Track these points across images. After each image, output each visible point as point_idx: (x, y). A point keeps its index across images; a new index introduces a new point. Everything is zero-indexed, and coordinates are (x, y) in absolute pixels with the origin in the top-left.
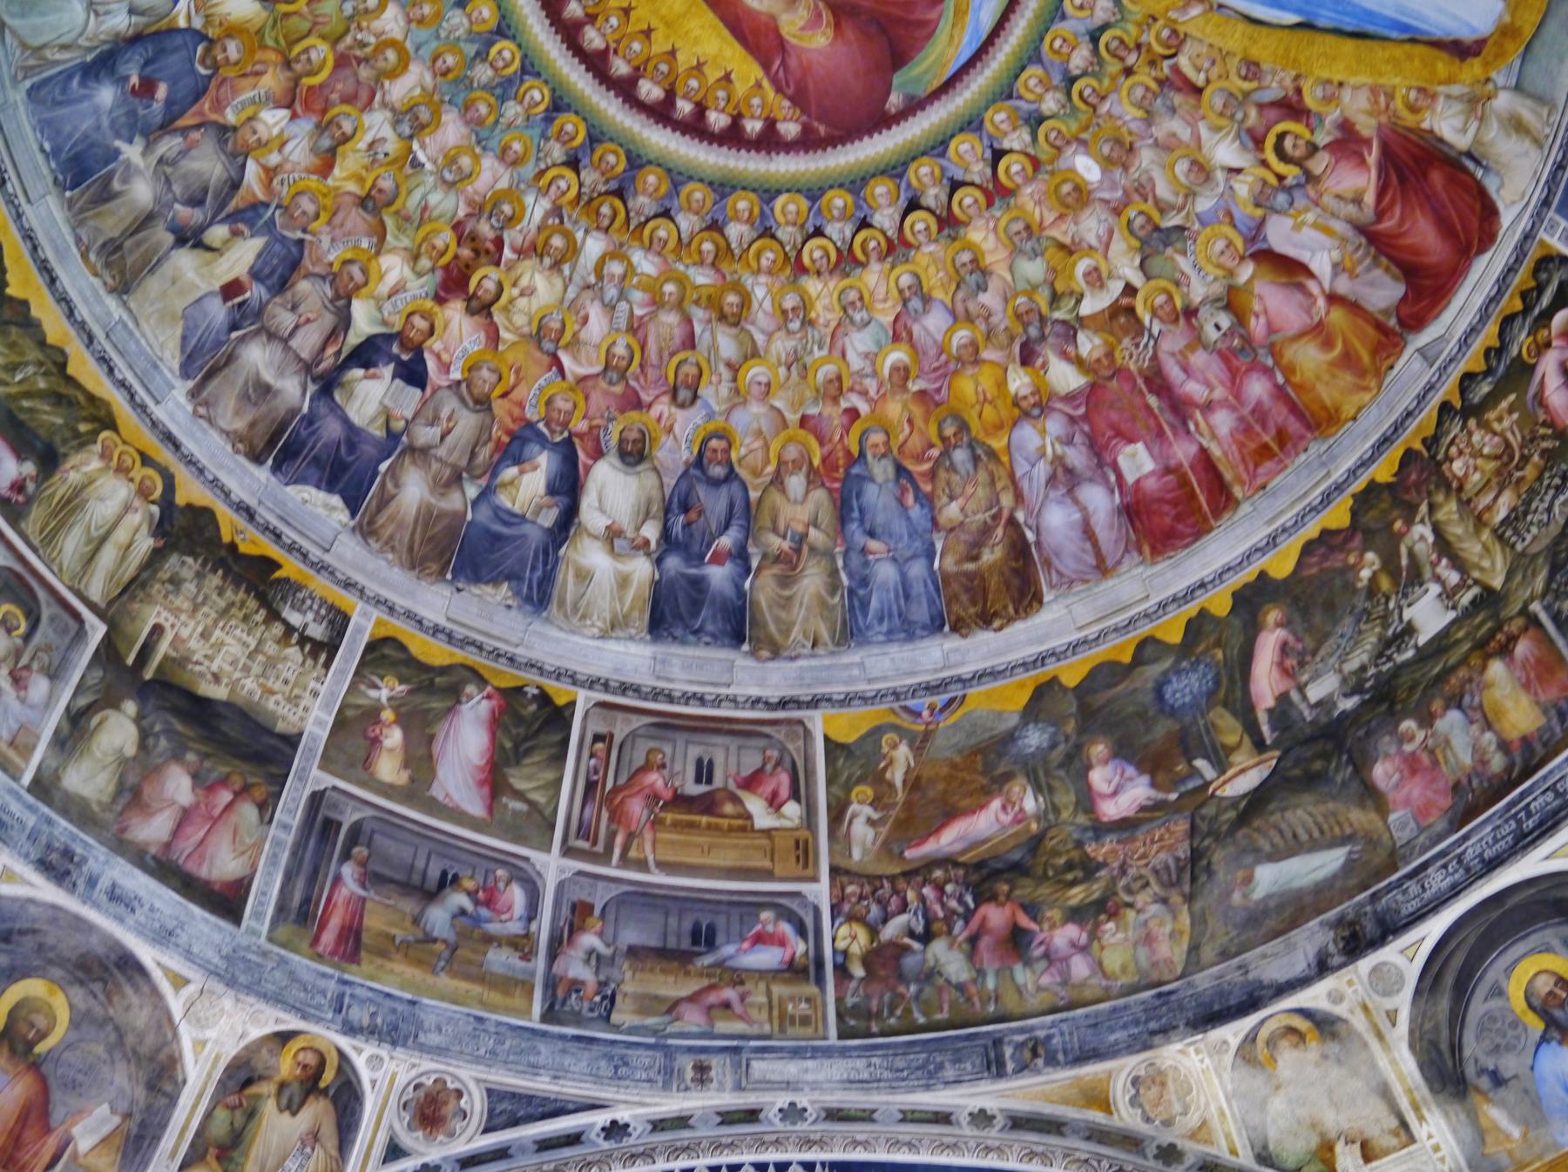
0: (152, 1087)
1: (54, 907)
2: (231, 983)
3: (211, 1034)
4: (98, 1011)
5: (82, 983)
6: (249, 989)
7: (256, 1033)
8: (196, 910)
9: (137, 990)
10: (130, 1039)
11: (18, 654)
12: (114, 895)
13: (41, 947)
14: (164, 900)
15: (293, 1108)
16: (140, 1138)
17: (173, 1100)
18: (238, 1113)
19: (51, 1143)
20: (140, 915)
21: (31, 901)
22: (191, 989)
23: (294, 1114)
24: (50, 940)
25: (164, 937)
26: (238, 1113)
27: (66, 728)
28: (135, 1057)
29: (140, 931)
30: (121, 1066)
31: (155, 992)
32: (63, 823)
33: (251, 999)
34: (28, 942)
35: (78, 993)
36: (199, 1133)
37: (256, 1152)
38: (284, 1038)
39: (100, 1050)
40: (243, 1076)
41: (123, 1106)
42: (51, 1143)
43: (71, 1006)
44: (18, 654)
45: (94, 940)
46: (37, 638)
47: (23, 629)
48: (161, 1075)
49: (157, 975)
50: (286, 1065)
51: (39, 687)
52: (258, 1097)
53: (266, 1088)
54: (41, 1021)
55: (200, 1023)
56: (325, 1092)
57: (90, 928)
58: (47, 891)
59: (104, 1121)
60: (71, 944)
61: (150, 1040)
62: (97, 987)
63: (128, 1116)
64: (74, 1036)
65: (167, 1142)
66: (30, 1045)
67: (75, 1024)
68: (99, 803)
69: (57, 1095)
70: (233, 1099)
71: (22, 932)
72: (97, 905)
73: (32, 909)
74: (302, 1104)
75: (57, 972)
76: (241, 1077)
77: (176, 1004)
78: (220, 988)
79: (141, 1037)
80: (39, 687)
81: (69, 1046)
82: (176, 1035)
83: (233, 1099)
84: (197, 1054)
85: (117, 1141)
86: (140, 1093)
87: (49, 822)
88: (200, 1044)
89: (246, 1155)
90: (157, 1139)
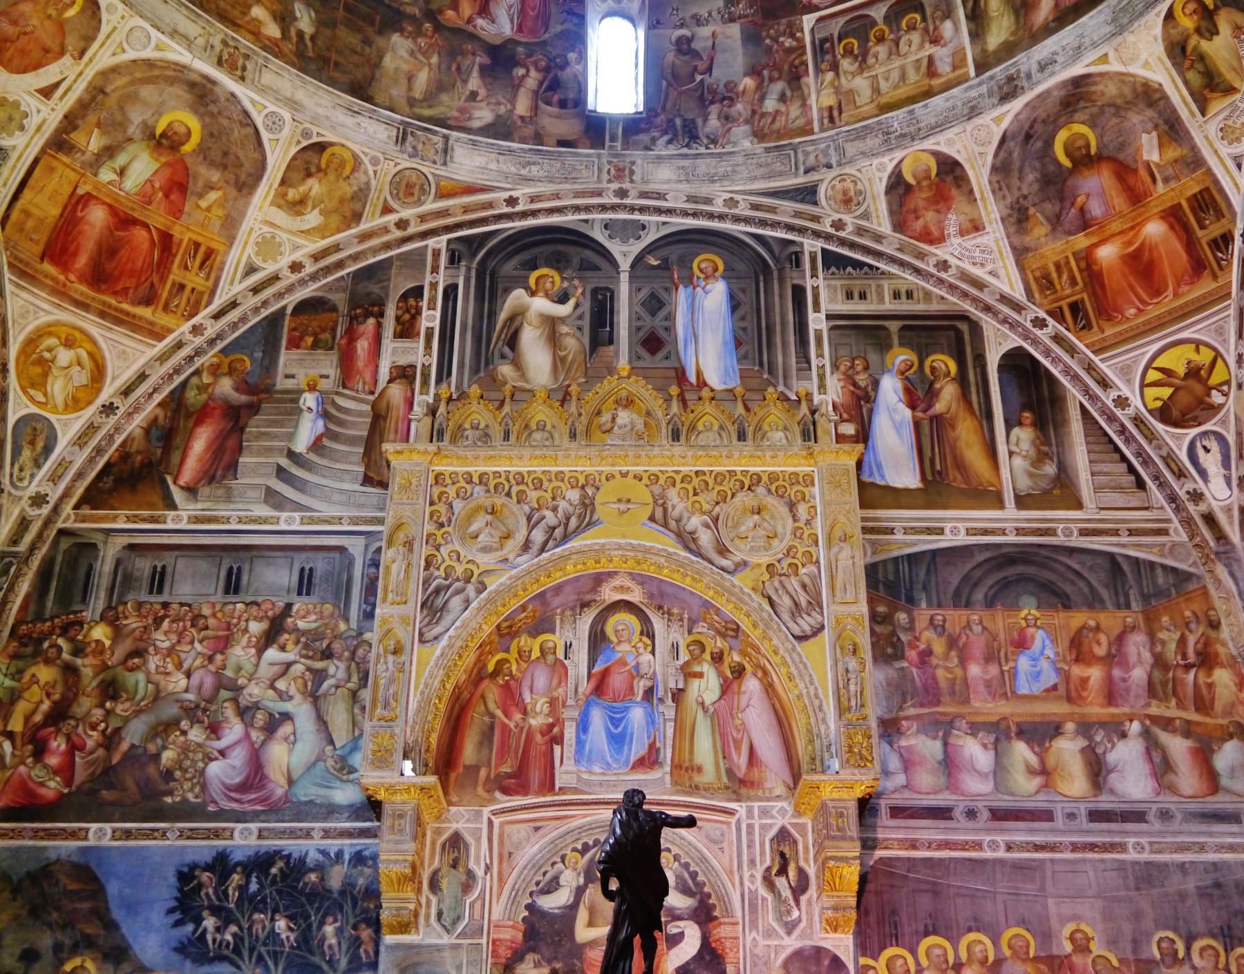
0: (1151, 104)
1: (1027, 105)
2: (1121, 30)
3: (1144, 56)
4: (1094, 110)
5: (1075, 111)
6: (1131, 22)
7: (1158, 30)
8: (1084, 19)
9: (1096, 84)
10: (1119, 102)
11: (926, 30)
12: (1042, 67)
13: (1044, 121)
14: (1066, 36)
15: (1214, 32)
16: (1172, 127)
17: (1165, 97)
18: (1197, 65)
19: (1143, 173)
20: (1060, 59)
21: (1017, 115)
22: (1111, 55)
23: (1217, 33)
24: (1044, 115)
25: (1078, 52)
26: (1197, 65)
27: (973, 26)
28: (1130, 105)
29: (1066, 66)
30: (1130, 115)
31: (1101, 75)
32: (998, 69)
33: (1136, 24)
34: (1038, 127)
35: (1078, 116)
36: (1192, 94)
37: (1223, 69)
38: (1170, 16)
39: (1115, 121)
40: (1178, 50)
41: (1150, 126)
42: (1143, 173)
43: (1083, 123)
44: (926, 30)
45: (1055, 93)
46: (928, 11)
47: (918, 16)
48: (1149, 95)
49: (1093, 69)
50: (1187, 22)
51: (947, 28)
52: (1195, 48)
53: (1194, 41)
54: (1080, 143)
55: (1134, 59)
56: (1217, 8)
57: (1047, 93)
58: (1017, 105)
59: (1150, 140)
60: (1051, 105)
61: (1127, 91)
62: (1082, 104)
63: (1156, 127)
64: (1098, 130)
65: (1184, 114)
66: (1088, 154)
67: (1093, 126)
68: (1012, 34)
69: (1121, 157)
70: (1187, 63)
71: (1031, 127)
72: (1039, 82)
73: (1022, 117)
74: (1215, 26)
75: (1062, 120)
76: (1178, 51)
77: (1115, 66)
78: (1119, 39)
79: (1122, 95)
80: (947, 28)
81: (1100, 137)
82: (1133, 76)
83: (1187, 63)
84: (1151, 69)
85: (1165, 139)
86: (1150, 113)
87: (992, 78)
88: (1146, 64)
89: (1220, 74)
90: (1178, 118)
